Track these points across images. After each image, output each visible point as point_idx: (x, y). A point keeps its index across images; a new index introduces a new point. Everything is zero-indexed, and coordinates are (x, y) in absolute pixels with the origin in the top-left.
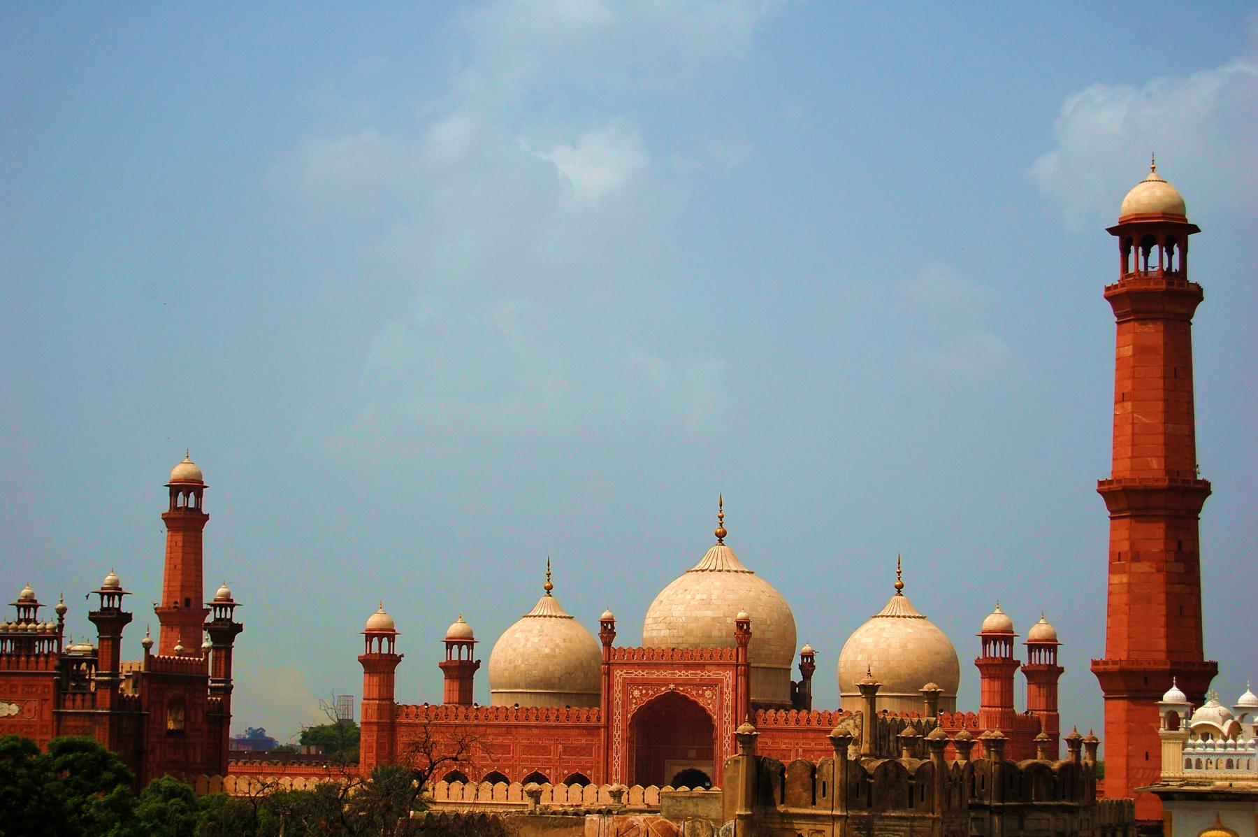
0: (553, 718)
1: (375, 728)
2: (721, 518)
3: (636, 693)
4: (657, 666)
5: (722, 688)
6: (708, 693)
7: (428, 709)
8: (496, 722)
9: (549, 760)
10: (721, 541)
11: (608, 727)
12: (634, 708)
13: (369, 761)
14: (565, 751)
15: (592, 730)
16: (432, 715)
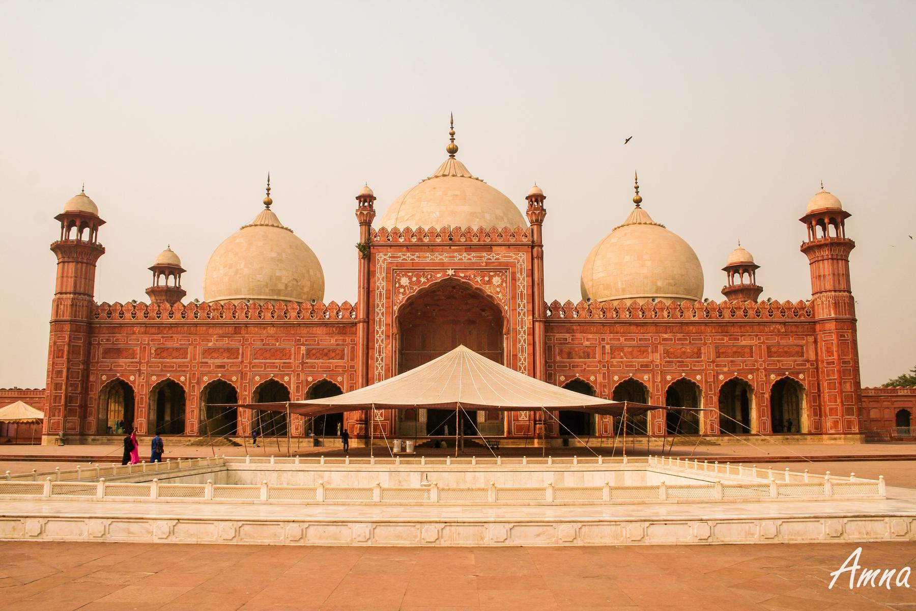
0: (293, 314)
1: (67, 327)
2: (452, 134)
3: (404, 281)
4: (431, 247)
5: (514, 274)
6: (496, 280)
7: (135, 306)
8: (220, 320)
9: (287, 365)
10: (452, 156)
11: (368, 320)
12: (401, 299)
13: (58, 368)
14: (309, 353)
15: (345, 328)
16: (140, 314)
